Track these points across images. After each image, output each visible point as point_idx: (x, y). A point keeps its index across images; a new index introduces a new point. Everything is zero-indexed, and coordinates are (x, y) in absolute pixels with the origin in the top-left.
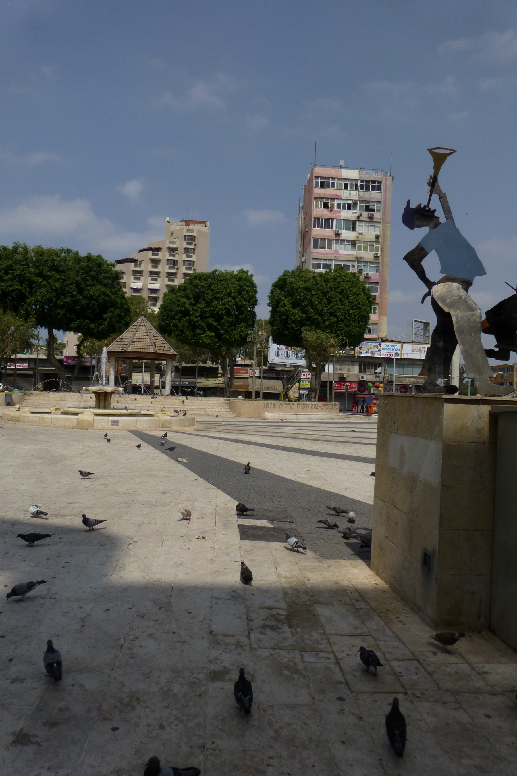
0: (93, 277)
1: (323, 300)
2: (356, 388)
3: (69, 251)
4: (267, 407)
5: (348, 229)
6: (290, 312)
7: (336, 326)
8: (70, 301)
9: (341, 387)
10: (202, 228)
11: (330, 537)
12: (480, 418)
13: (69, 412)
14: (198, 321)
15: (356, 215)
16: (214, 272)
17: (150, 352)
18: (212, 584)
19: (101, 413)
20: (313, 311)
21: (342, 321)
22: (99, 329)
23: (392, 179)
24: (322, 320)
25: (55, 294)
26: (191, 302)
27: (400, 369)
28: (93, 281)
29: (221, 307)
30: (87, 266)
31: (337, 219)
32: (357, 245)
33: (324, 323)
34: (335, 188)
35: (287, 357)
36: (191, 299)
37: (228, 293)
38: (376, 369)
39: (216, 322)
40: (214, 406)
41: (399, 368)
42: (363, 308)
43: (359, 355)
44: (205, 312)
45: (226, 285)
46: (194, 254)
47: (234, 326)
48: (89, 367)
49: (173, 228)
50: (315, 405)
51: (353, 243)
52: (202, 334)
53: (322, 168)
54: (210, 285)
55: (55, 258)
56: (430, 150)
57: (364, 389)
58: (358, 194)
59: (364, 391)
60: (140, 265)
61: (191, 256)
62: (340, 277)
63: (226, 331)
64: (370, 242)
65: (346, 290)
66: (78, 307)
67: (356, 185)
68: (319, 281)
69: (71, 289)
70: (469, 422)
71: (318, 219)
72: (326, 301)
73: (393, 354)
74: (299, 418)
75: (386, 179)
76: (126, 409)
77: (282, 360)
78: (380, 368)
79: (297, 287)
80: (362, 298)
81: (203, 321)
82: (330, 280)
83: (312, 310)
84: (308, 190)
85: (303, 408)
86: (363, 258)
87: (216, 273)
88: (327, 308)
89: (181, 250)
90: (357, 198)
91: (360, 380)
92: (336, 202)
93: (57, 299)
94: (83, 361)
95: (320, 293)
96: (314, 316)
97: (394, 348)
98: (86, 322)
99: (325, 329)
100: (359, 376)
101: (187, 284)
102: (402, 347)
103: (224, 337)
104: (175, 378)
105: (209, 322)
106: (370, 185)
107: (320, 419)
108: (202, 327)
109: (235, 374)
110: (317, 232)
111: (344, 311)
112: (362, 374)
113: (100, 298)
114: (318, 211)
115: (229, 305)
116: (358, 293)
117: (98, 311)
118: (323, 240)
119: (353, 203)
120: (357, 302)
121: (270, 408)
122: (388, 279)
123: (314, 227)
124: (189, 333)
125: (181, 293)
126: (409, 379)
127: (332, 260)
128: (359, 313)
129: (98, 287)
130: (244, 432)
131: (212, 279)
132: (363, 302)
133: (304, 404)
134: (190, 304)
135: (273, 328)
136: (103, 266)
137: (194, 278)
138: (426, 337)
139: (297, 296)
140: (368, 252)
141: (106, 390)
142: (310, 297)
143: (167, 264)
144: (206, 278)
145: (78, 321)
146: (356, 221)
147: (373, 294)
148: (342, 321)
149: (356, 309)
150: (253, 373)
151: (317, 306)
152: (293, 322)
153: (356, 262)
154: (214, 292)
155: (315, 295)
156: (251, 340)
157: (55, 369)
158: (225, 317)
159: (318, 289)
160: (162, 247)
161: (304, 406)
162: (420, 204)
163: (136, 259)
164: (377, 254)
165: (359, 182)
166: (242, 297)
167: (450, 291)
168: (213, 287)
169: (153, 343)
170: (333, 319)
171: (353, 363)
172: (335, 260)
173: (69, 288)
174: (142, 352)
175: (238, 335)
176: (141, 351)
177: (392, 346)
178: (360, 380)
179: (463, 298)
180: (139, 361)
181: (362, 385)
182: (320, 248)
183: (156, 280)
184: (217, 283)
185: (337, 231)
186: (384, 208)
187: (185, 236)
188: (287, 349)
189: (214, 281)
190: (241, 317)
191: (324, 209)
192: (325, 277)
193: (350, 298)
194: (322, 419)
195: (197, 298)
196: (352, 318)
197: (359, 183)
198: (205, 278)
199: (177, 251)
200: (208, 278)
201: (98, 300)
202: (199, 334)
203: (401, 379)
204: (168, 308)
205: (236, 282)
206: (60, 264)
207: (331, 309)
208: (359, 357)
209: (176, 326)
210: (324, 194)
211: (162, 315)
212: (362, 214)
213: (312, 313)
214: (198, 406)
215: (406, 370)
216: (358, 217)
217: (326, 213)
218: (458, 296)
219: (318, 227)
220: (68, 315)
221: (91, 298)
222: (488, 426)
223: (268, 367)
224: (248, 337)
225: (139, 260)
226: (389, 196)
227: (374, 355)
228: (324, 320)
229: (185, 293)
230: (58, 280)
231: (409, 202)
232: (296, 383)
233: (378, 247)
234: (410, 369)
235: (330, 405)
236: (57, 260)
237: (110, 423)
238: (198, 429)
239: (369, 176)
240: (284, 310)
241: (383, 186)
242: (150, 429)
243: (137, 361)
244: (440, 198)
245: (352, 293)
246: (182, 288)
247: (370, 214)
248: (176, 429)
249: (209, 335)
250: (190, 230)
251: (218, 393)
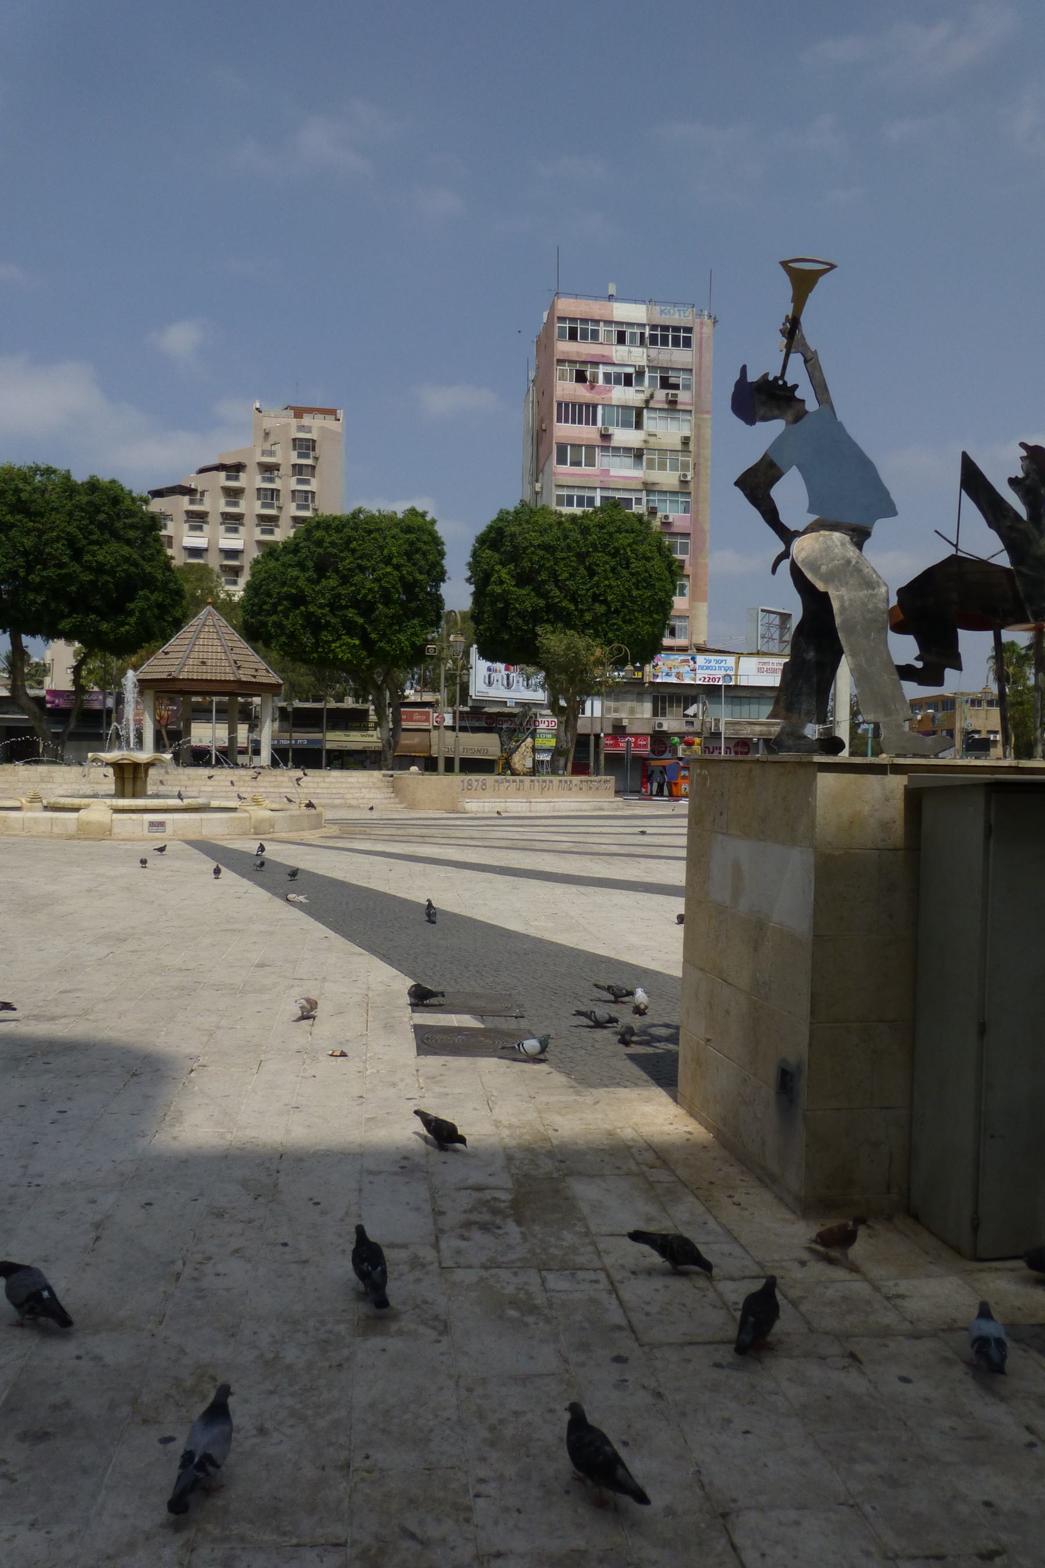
0: (102, 526)
1: (578, 570)
2: (647, 747)
3: (49, 471)
4: (470, 787)
5: (626, 424)
6: (512, 594)
7: (607, 623)
8: (57, 576)
9: (618, 746)
10: (329, 423)
11: (597, 1045)
12: (887, 800)
13: (59, 806)
14: (324, 615)
15: (642, 397)
16: (355, 515)
17: (228, 679)
18: (361, 1145)
19: (127, 806)
20: (558, 593)
21: (617, 612)
22: (118, 633)
23: (714, 323)
24: (576, 609)
25: (25, 562)
26: (309, 576)
28: (102, 534)
29: (372, 585)
30: (87, 502)
31: (604, 405)
32: (645, 457)
33: (582, 616)
34: (600, 341)
35: (509, 686)
36: (309, 569)
37: (385, 557)
38: (686, 709)
39: (361, 616)
40: (360, 788)
41: (732, 704)
42: (658, 584)
43: (652, 680)
44: (338, 596)
45: (380, 540)
46: (314, 477)
47: (400, 625)
48: (100, 711)
49: (268, 423)
50: (566, 782)
51: (638, 454)
52: (334, 641)
53: (572, 300)
54: (349, 541)
55: (21, 486)
56: (784, 264)
57: (663, 749)
58: (645, 355)
59: (663, 752)
60: (201, 500)
61: (306, 482)
62: (612, 523)
63: (383, 636)
64: (671, 451)
65: (624, 549)
66: (74, 588)
67: (642, 335)
68: (571, 531)
69: (56, 550)
70: (867, 809)
71: (567, 405)
72: (586, 573)
73: (719, 678)
74: (533, 809)
75: (702, 324)
76: (180, 796)
77: (498, 692)
78: (695, 706)
79: (526, 544)
80: (657, 565)
81: (335, 615)
82: (592, 530)
83: (557, 591)
84: (544, 344)
85: (543, 789)
86: (657, 483)
87: (361, 515)
88: (588, 586)
89: (286, 470)
90: (644, 363)
91: (655, 731)
92: (602, 370)
93: (28, 573)
94: (86, 700)
95: (573, 556)
96: (560, 602)
97: (721, 665)
98: (91, 619)
99: (583, 629)
100: (652, 722)
101: (299, 538)
102: (737, 663)
103: (380, 647)
104: (280, 731)
105: (346, 616)
106: (670, 336)
107: (577, 810)
108: (334, 627)
109: (403, 723)
110: (565, 431)
111: (620, 591)
112: (659, 718)
113: (119, 569)
114: (566, 389)
115: (387, 582)
116: (649, 555)
117: (114, 595)
118: (576, 447)
119: (636, 372)
120: (647, 575)
121: (476, 790)
122: (707, 527)
123: (558, 422)
124: (308, 639)
125: (288, 558)
126: (753, 726)
127: (596, 488)
128: (650, 595)
129: (114, 546)
130: (423, 839)
131: (352, 529)
132: (658, 574)
133: (544, 781)
134: (308, 580)
135: (478, 629)
136: (123, 502)
137: (315, 526)
138: (785, 642)
139: (526, 562)
140: (668, 471)
141: (137, 758)
142: (552, 563)
143: (259, 499)
144: (340, 527)
145: (75, 618)
146: (643, 408)
147: (678, 556)
148: (617, 612)
149: (645, 588)
150: (438, 720)
151: (567, 583)
152: (521, 614)
153: (644, 492)
154: (357, 555)
155: (563, 559)
156: (435, 652)
157: (27, 717)
158: (380, 606)
159: (569, 548)
160: (247, 464)
161: (544, 784)
162: (767, 374)
163: (193, 487)
164: (685, 476)
165: (647, 328)
166: (414, 564)
167: (827, 549)
168: (353, 545)
169: (232, 662)
170: (600, 609)
171: (640, 697)
172: (601, 488)
173: (52, 548)
174: (211, 680)
175: (406, 642)
176: (209, 678)
177: (717, 662)
178: (655, 731)
179: (854, 562)
180: (205, 699)
181: (660, 740)
182: (572, 464)
183: (235, 530)
184: (363, 536)
185: (605, 428)
186: (699, 383)
187: (294, 440)
188: (507, 669)
189: (356, 532)
190: (413, 605)
191: (579, 385)
192: (582, 523)
193: (633, 566)
194: (581, 811)
195: (321, 569)
196: (638, 605)
197: (647, 332)
198: (337, 526)
199: (278, 470)
200: (344, 526)
201: (116, 572)
202: (327, 642)
203: (737, 727)
204: (262, 591)
205: (401, 535)
206: (33, 498)
207: (595, 589)
208: (652, 683)
209: (279, 625)
210: (577, 353)
211: (252, 604)
212: (655, 395)
213: (557, 597)
214: (328, 788)
215: (746, 708)
216: (647, 402)
217: (581, 393)
218: (843, 558)
219: (566, 421)
220: (53, 606)
221: (100, 569)
222: (903, 815)
223: (470, 707)
224: (429, 646)
225: (200, 490)
226: (708, 357)
227: (683, 680)
228: (582, 611)
229: (296, 559)
230: (28, 532)
231: (744, 370)
232: (527, 738)
233: (688, 463)
234: (754, 708)
235: (595, 781)
236: (25, 491)
237: (146, 825)
238: (328, 835)
239: (668, 316)
240: (499, 591)
241: (694, 337)
242: (229, 837)
243: (199, 699)
244: (806, 361)
245: (637, 555)
246: (292, 548)
247: (670, 395)
248: (283, 835)
249: (347, 644)
250: (303, 426)
251: (368, 761)
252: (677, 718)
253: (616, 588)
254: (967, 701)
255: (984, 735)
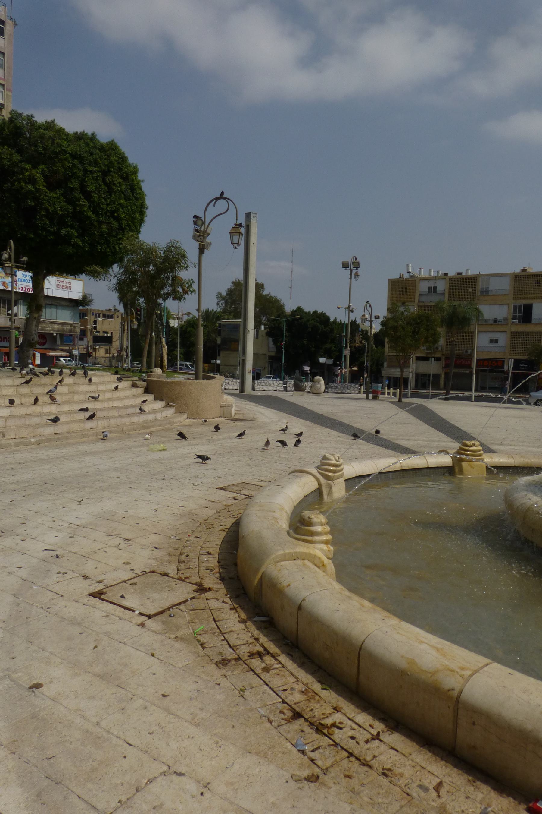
27: (58, 310)
33: (100, 227)
95: (99, 172)
111: (128, 211)
126: (53, 325)
155: (91, 172)
170: (115, 224)
213: (84, 206)
228: (100, 223)
252: (3, 316)
253: (126, 208)
254: (93, 314)
255: (101, 334)
